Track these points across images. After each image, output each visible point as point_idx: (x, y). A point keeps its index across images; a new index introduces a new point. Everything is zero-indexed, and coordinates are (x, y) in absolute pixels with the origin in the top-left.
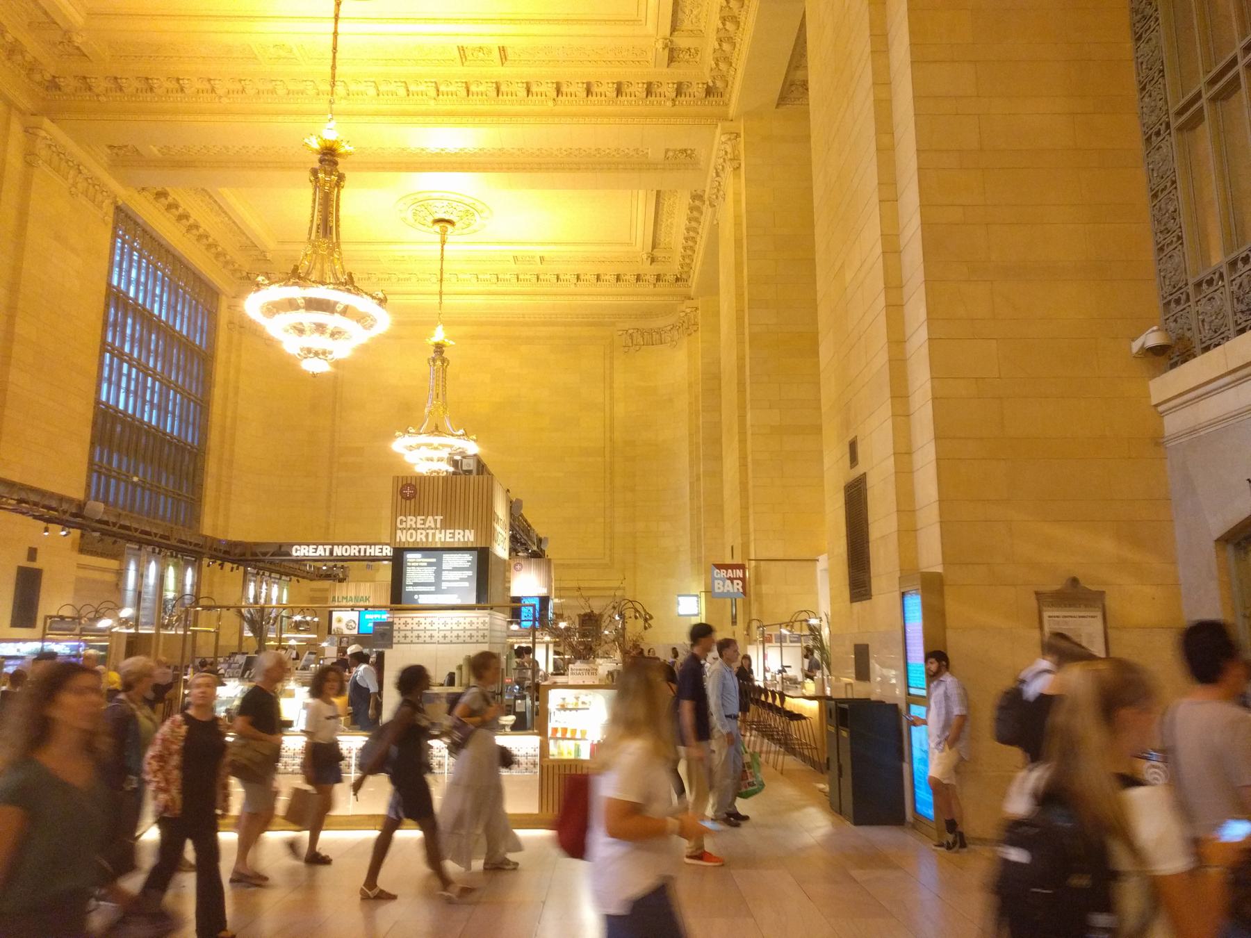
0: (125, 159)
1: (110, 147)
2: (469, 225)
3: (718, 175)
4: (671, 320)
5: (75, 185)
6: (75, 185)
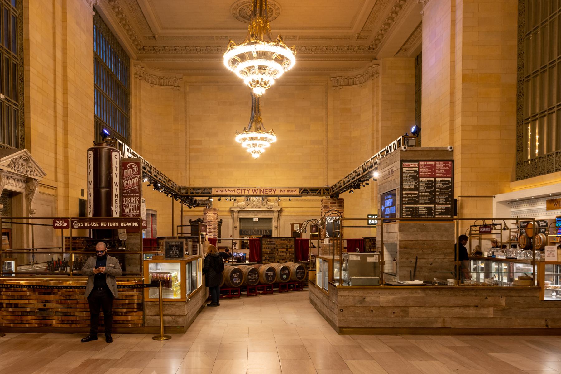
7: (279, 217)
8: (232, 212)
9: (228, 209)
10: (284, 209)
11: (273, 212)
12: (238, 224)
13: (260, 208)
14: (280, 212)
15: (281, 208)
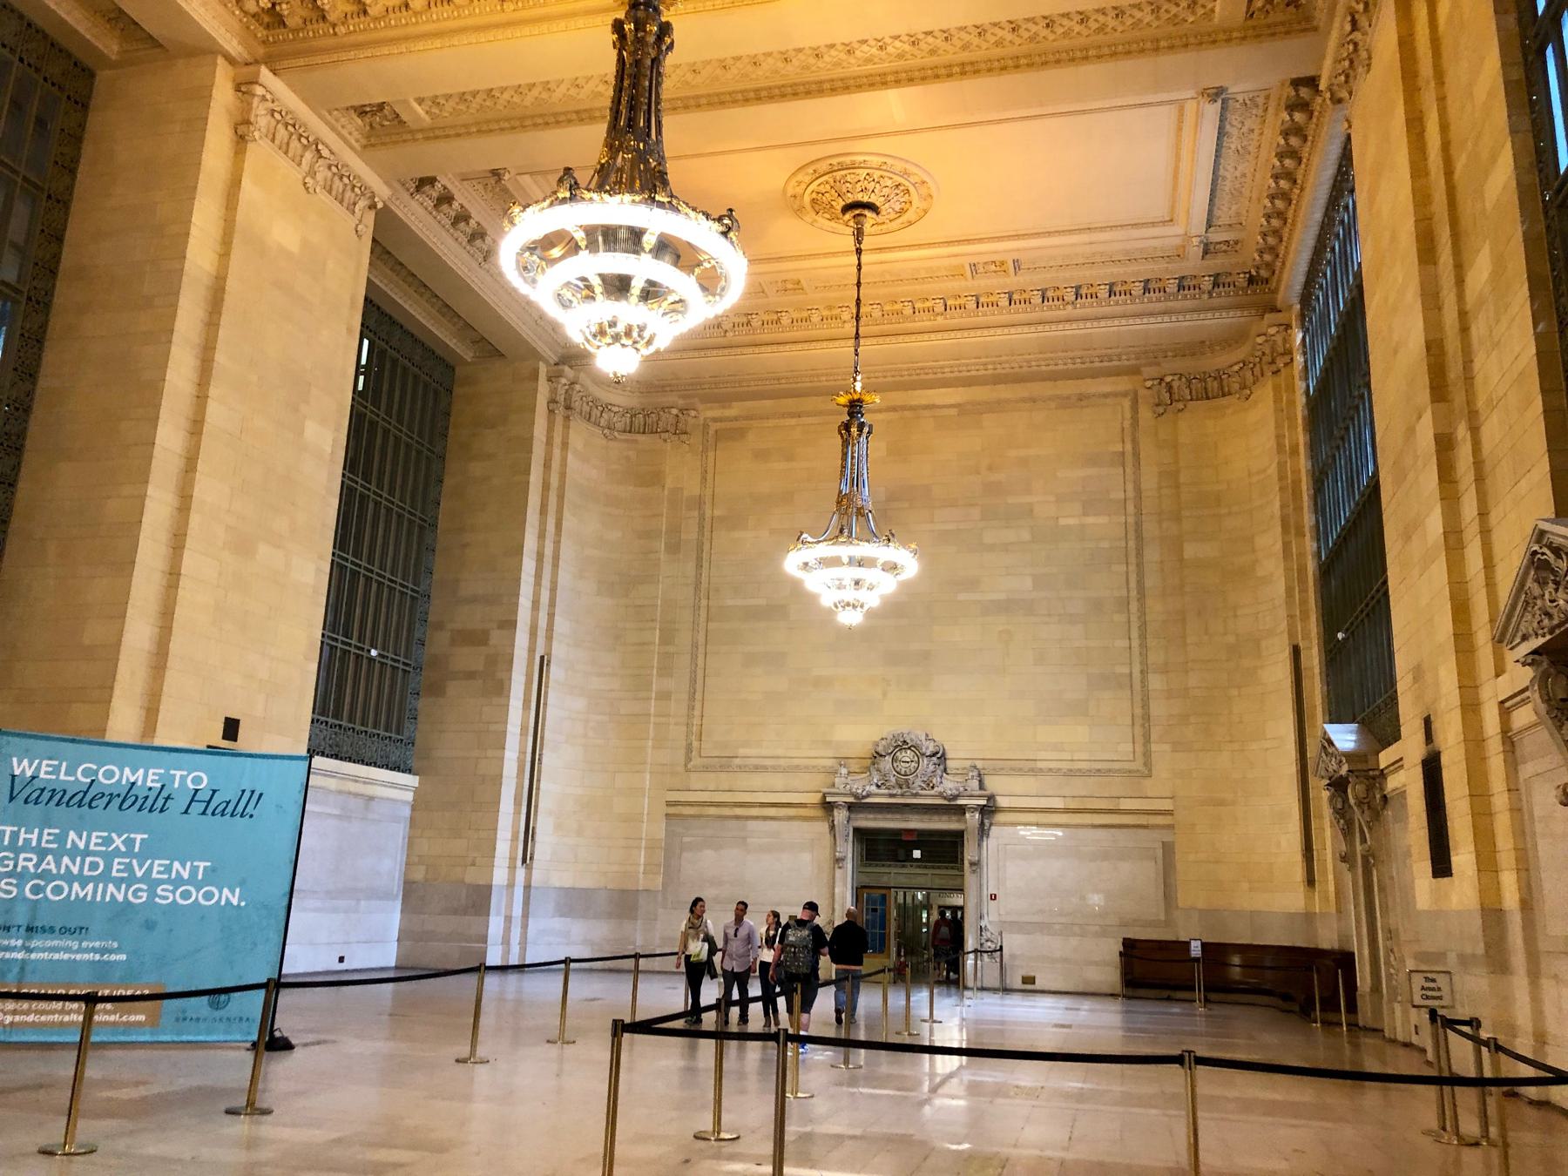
0: (379, 122)
1: (361, 111)
2: (902, 212)
3: (1354, 23)
4: (1241, 353)
5: (312, 173)
6: (312, 173)
7: (983, 832)
8: (828, 807)
9: (815, 798)
10: (1002, 802)
11: (961, 810)
12: (847, 849)
13: (916, 795)
14: (989, 810)
15: (991, 798)
